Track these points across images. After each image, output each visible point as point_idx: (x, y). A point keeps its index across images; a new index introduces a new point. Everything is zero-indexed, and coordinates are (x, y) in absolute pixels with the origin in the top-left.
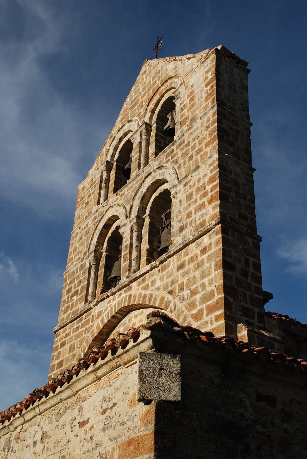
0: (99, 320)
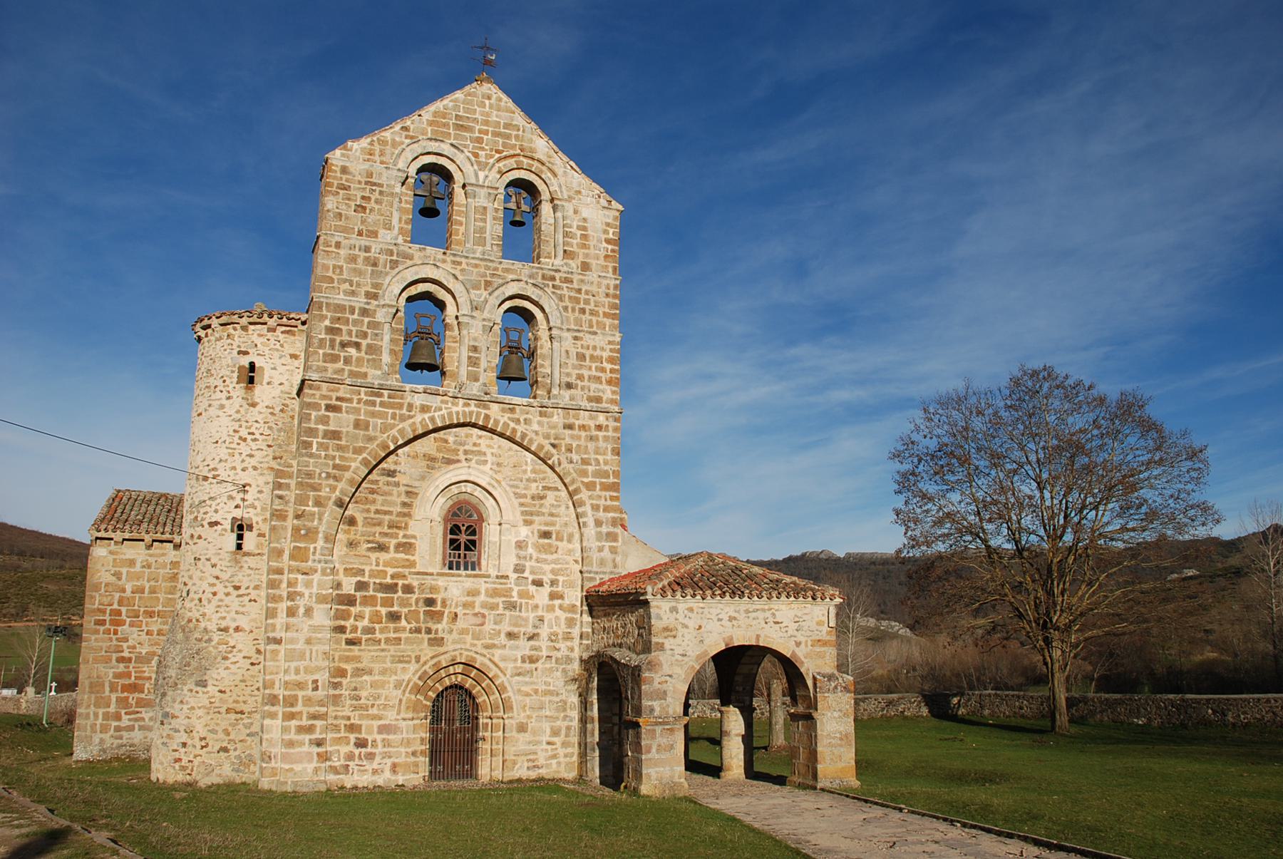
0: (426, 416)
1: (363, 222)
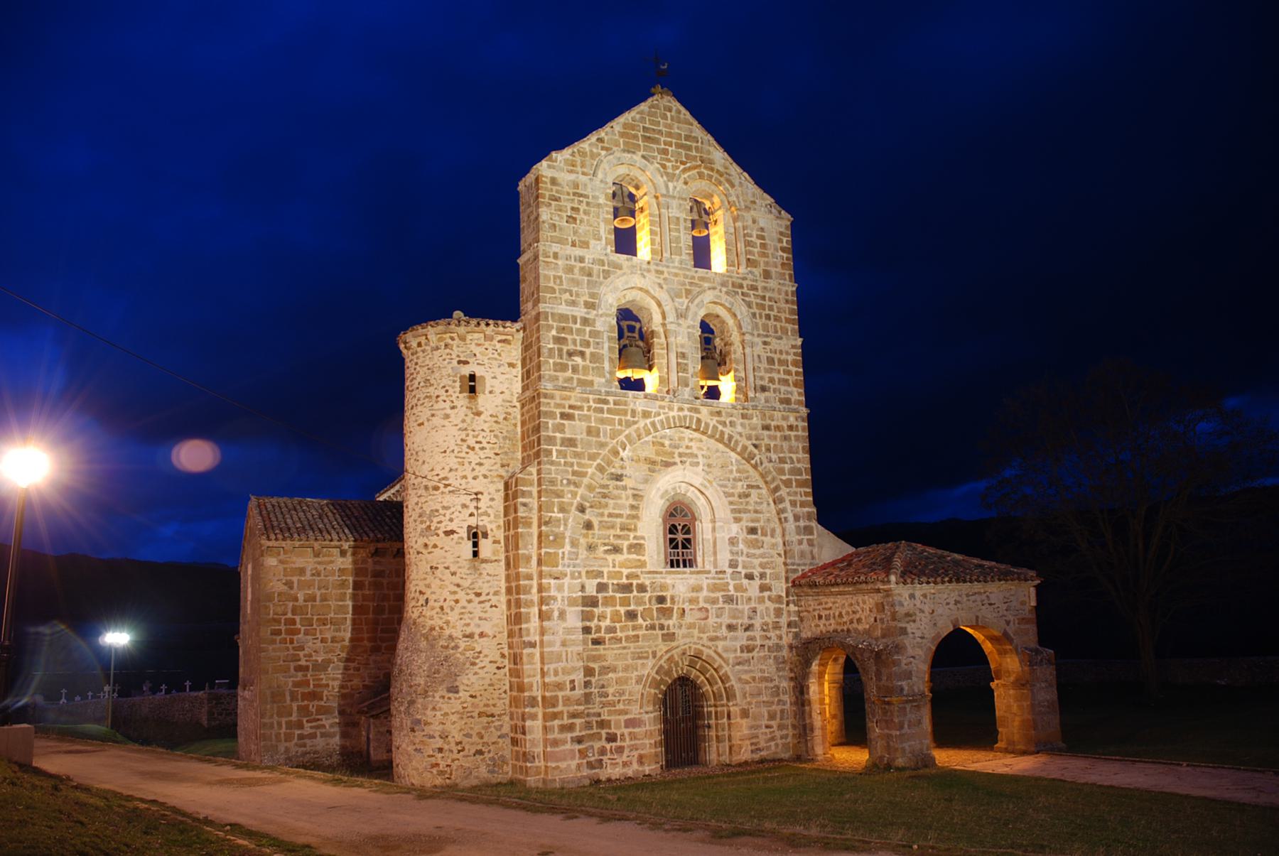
0: (648, 421)
1: (575, 233)
